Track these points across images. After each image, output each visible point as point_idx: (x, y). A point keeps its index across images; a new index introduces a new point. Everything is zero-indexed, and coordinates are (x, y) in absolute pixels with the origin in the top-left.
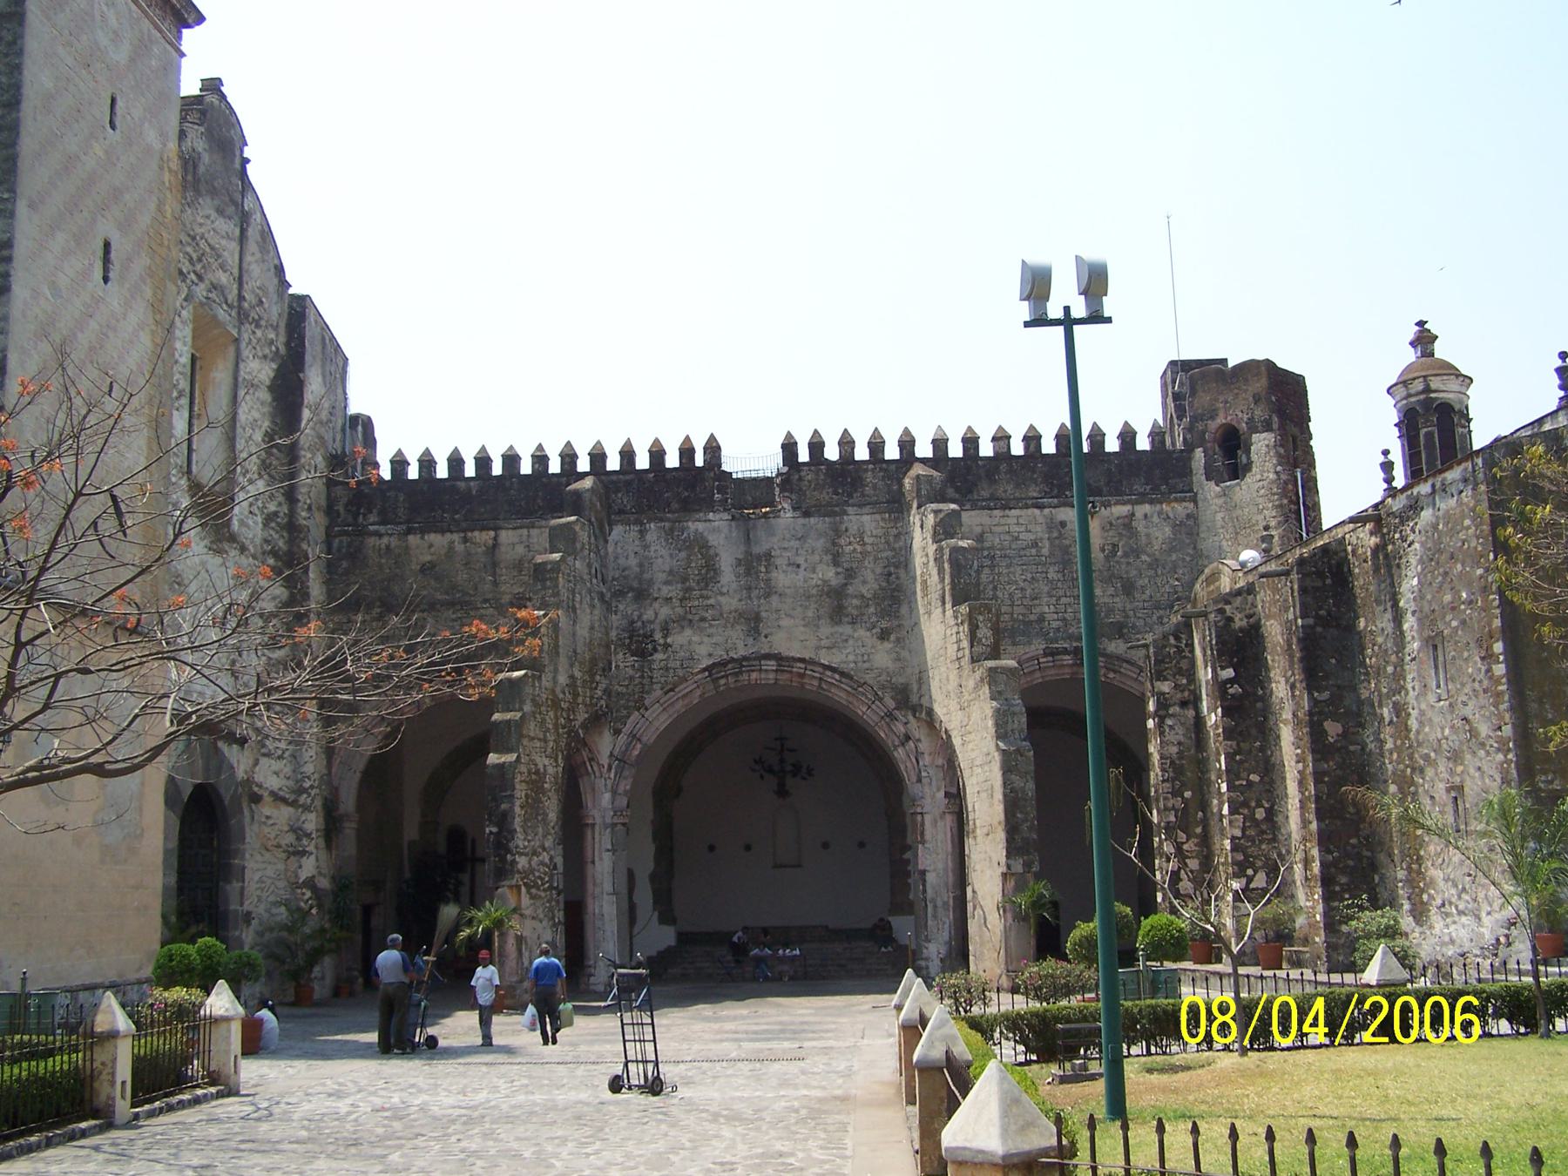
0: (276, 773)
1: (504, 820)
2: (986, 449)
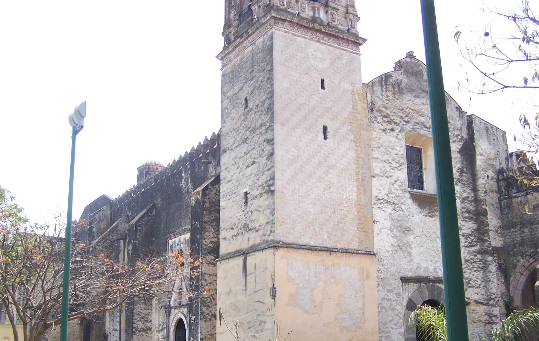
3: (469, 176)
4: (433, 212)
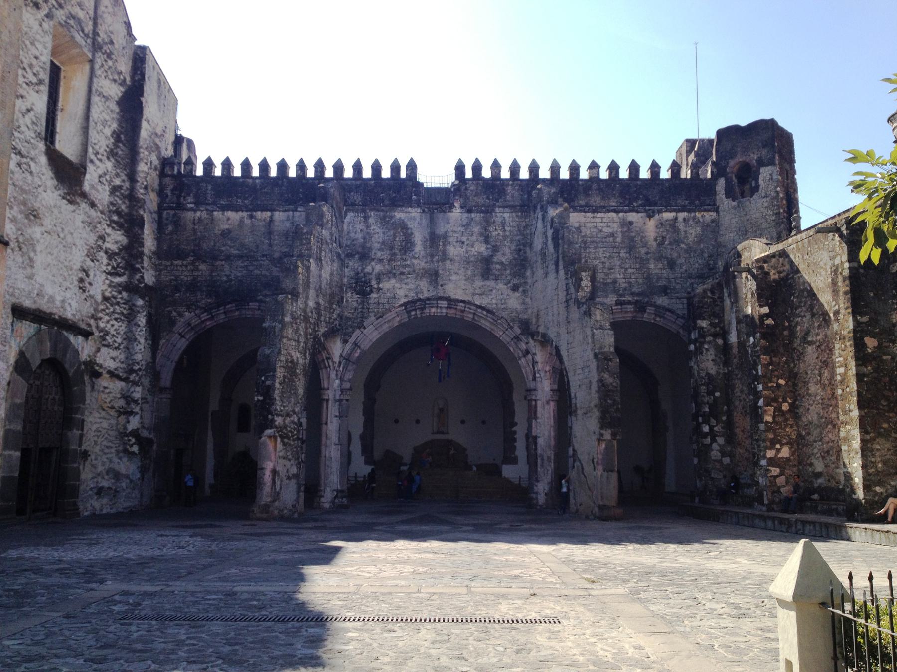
0: (113, 359)
1: (267, 392)
2: (584, 174)
3: (127, 151)
4: (74, 195)
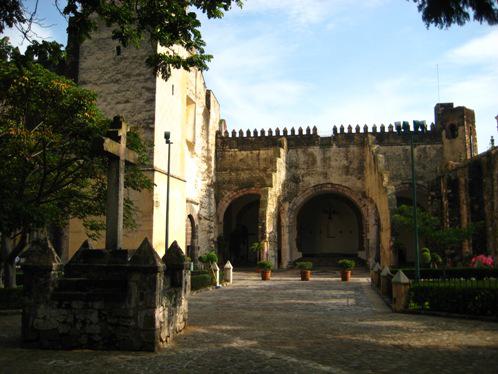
2: (387, 130)
